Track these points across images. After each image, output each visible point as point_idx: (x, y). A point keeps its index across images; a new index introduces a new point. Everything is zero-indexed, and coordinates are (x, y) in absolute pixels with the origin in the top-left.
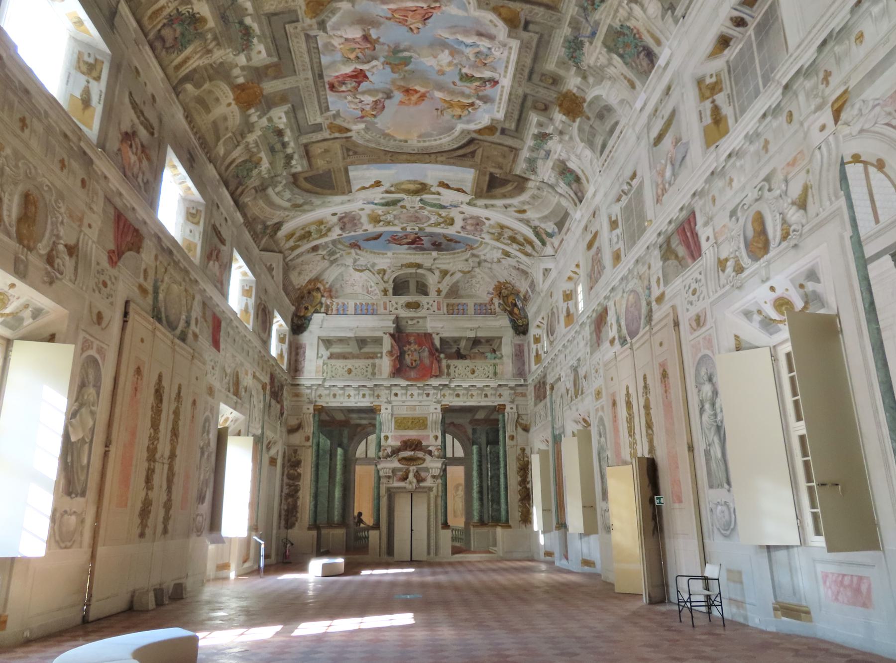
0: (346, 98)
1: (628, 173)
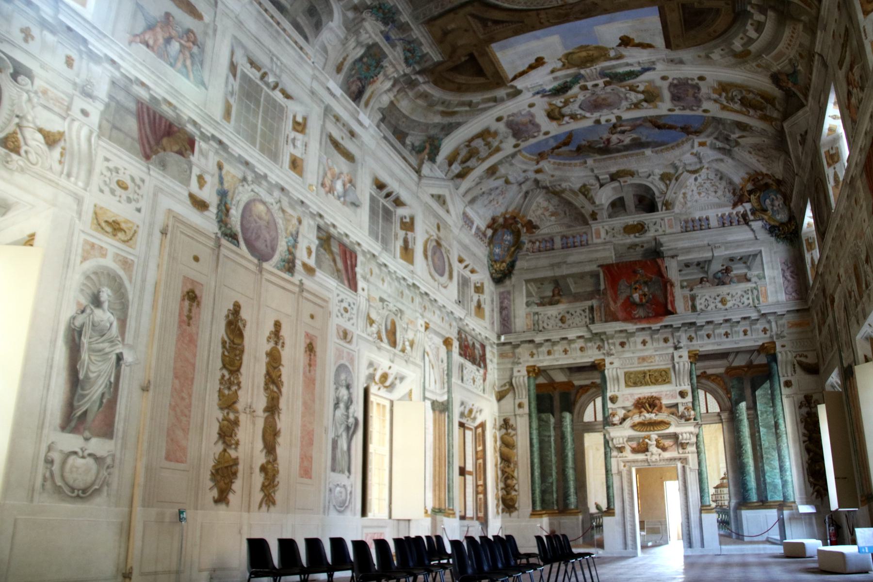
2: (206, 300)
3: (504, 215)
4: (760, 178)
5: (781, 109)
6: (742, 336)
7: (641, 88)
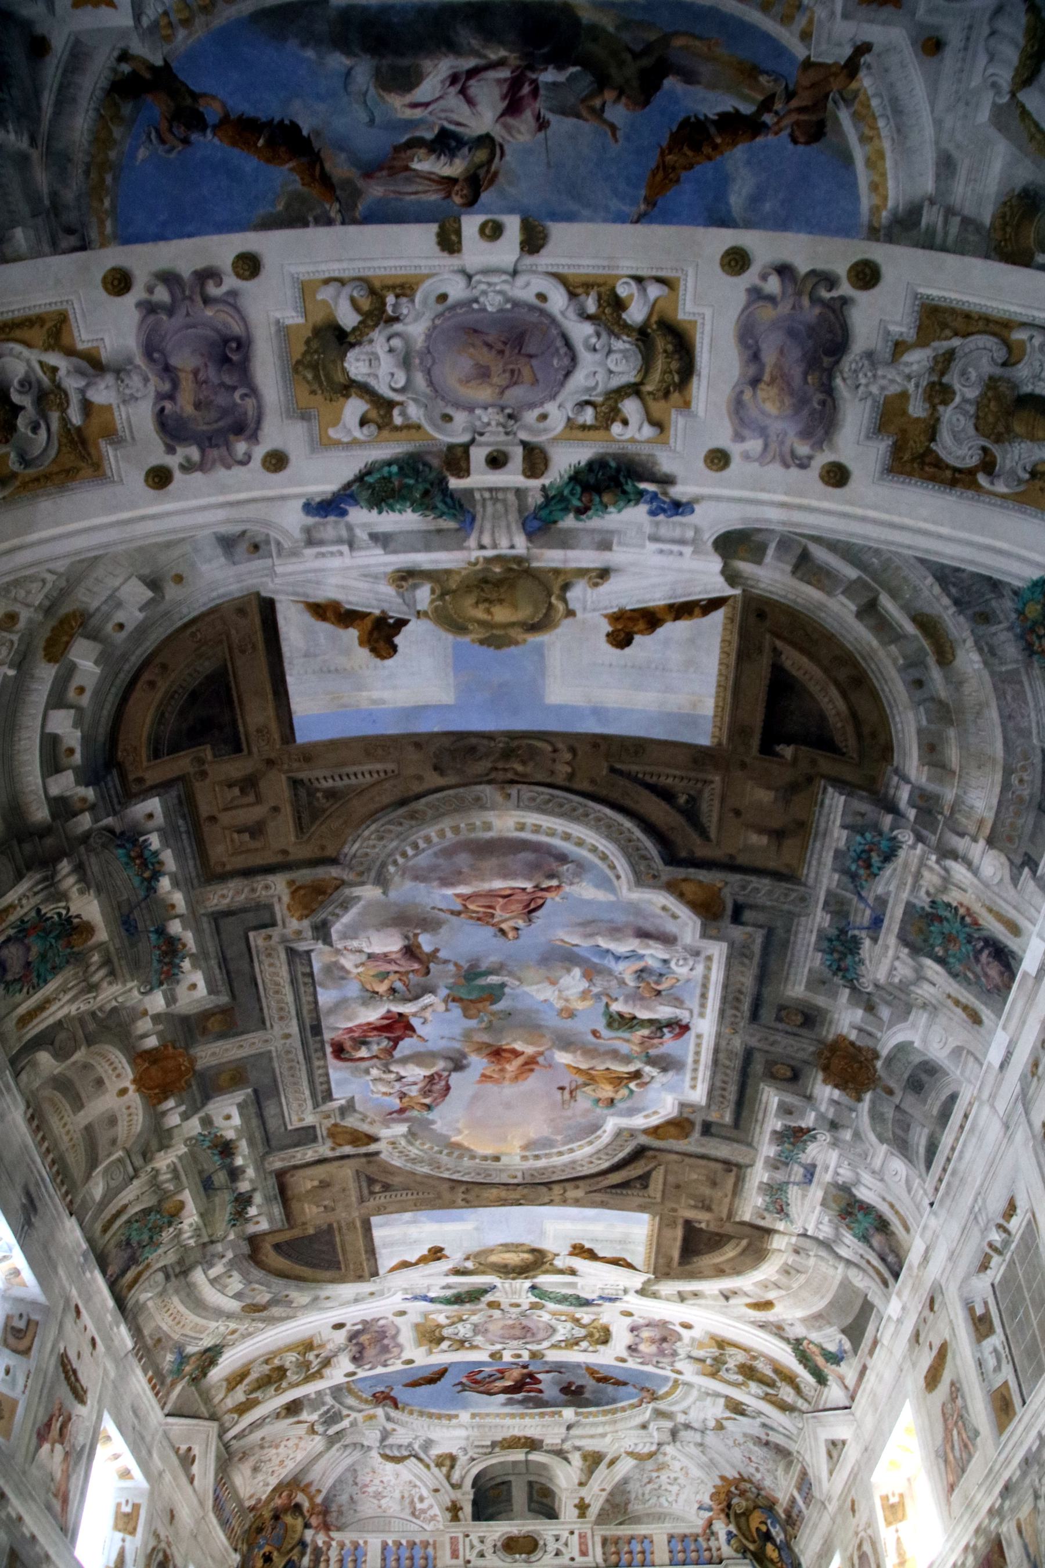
0: (367, 1072)
1: (996, 1205)
7: (355, 407)
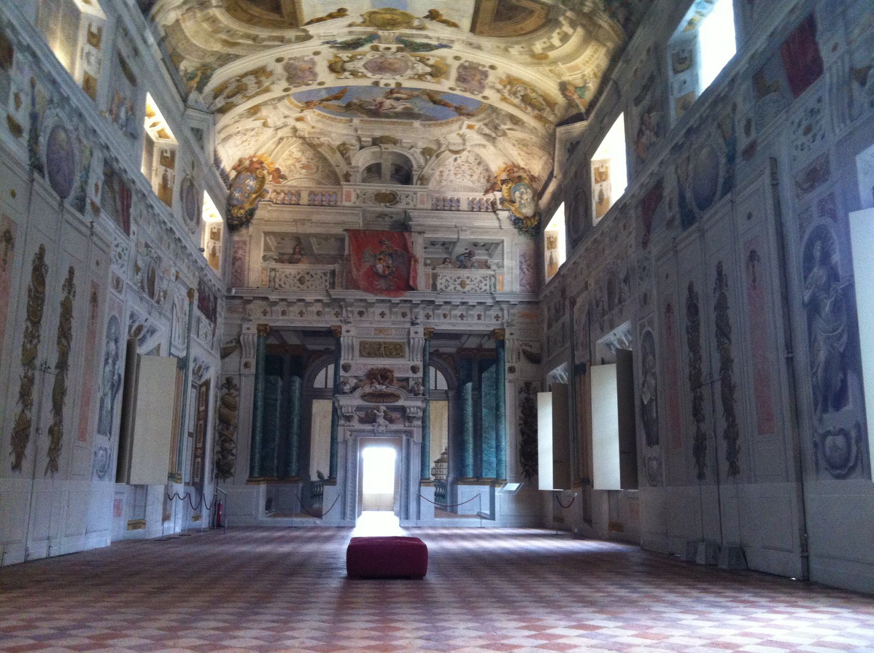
2: (19, 243)
3: (251, 158)
4: (515, 170)
5: (559, 115)
6: (476, 321)
7: (431, 62)
